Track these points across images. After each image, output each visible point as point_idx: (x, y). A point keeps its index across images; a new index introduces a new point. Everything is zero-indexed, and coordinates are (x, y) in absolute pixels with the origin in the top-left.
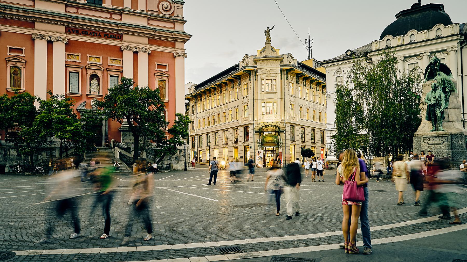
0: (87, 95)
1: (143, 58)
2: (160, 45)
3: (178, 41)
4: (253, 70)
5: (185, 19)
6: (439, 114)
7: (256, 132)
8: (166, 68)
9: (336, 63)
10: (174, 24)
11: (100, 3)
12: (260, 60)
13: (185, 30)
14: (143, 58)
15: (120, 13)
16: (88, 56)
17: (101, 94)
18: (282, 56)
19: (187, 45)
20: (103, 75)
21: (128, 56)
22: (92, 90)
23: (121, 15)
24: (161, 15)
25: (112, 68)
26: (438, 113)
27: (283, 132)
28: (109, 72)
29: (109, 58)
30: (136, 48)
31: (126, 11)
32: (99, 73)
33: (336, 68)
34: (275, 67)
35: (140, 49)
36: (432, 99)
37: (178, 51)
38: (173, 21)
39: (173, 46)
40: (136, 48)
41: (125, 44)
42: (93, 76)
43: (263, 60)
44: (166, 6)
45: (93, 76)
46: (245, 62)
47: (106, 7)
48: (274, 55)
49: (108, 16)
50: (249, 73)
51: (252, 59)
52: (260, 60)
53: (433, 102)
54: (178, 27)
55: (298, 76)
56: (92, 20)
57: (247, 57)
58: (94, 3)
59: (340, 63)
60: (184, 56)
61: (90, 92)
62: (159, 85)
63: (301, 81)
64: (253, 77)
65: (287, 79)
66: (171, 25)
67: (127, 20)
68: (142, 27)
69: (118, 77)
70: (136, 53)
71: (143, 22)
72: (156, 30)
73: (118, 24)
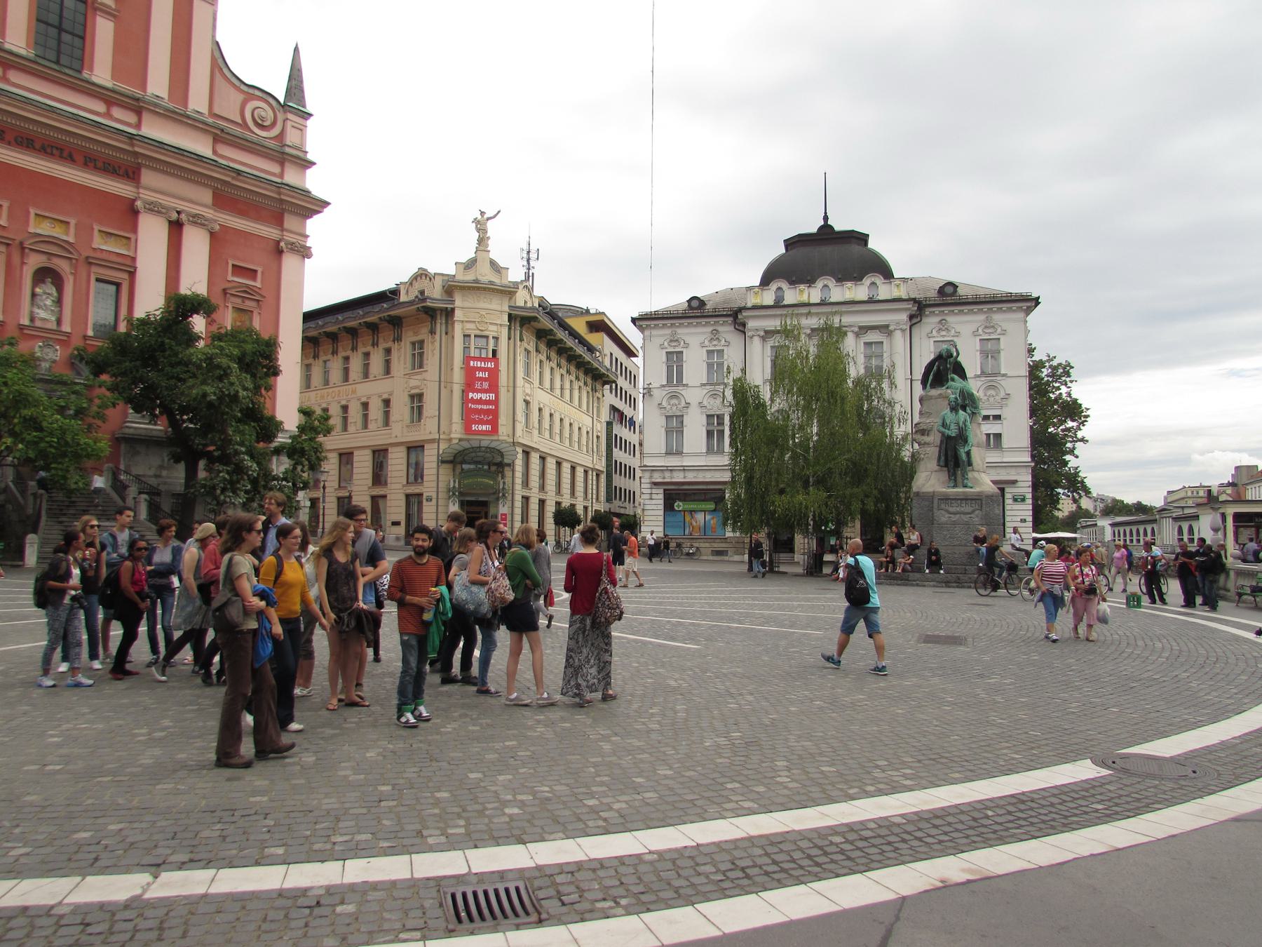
0: (21, 328)
1: (196, 246)
2: (243, 213)
3: (291, 212)
4: (441, 310)
5: (310, 157)
6: (964, 457)
7: (443, 462)
8: (254, 279)
9: (669, 322)
10: (282, 164)
11: (76, 65)
12: (462, 288)
14: (196, 246)
16: (32, 211)
17: (66, 328)
18: (516, 285)
19: (315, 227)
20: (74, 274)
22: (42, 314)
23: (139, 112)
24: (248, 135)
25: (104, 256)
26: (962, 452)
27: (509, 465)
28: (94, 269)
29: (96, 227)
30: (179, 213)
31: (156, 105)
32: (63, 266)
33: (668, 331)
34: (499, 308)
35: (189, 214)
36: (953, 426)
37: (290, 237)
39: (278, 220)
40: (179, 213)
41: (146, 195)
42: (44, 274)
43: (469, 288)
44: (263, 114)
45: (44, 274)
46: (418, 286)
47: (95, 79)
48: (497, 281)
49: (100, 107)
51: (438, 283)
52: (462, 288)
53: (953, 432)
55: (541, 334)
56: (53, 110)
57: (422, 274)
58: (58, 62)
59: (677, 322)
60: (305, 253)
61: (32, 319)
62: (234, 320)
63: (543, 347)
65: (521, 340)
66: (275, 168)
67: (153, 129)
68: (199, 158)
69: (118, 285)
70: (176, 228)
71: (201, 146)
72: (238, 172)
73: (131, 137)
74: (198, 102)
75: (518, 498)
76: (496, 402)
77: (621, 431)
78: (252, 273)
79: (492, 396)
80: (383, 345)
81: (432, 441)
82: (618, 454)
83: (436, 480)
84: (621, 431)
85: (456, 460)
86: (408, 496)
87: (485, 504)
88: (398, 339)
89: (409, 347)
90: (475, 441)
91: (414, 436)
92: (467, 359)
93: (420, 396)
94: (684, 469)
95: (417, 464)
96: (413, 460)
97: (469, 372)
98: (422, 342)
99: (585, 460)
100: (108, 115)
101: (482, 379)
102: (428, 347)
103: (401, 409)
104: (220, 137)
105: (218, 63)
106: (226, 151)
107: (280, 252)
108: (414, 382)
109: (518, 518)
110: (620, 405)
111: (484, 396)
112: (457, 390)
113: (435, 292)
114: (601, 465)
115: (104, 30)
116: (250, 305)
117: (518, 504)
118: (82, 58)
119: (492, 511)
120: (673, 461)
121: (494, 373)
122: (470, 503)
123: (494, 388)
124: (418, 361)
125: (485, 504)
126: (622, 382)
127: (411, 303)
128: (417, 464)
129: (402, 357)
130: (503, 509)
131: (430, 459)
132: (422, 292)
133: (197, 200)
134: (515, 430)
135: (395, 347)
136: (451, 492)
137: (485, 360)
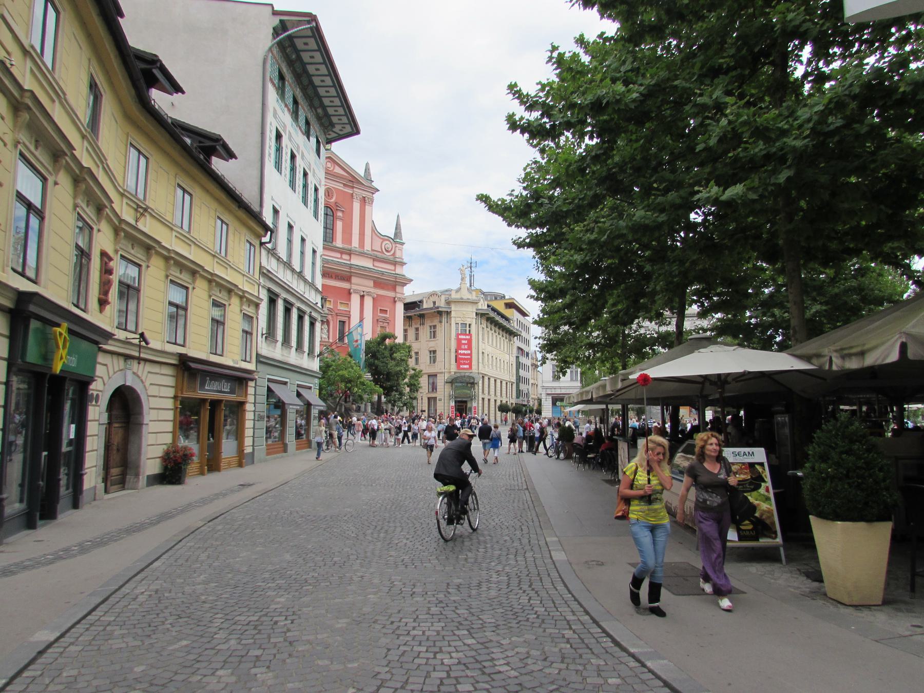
1: (368, 302)
2: (383, 288)
5: (405, 261)
13: (404, 273)
14: (368, 302)
15: (350, 253)
21: (355, 299)
23: (350, 255)
37: (398, 295)
38: (395, 263)
39: (394, 289)
41: (354, 287)
46: (432, 299)
49: (338, 255)
50: (440, 313)
51: (443, 298)
54: (399, 270)
57: (433, 294)
63: (489, 325)
64: (444, 319)
66: (393, 268)
67: (356, 261)
70: (362, 297)
71: (368, 264)
74: (367, 247)
75: (480, 399)
76: (471, 355)
77: (523, 360)
78: (385, 311)
79: (469, 352)
80: (414, 326)
81: (441, 373)
82: (522, 373)
83: (444, 393)
84: (523, 360)
85: (452, 382)
86: (429, 399)
87: (466, 402)
88: (423, 324)
89: (428, 328)
90: (463, 373)
91: (432, 370)
92: (458, 335)
93: (434, 352)
94: (560, 388)
95: (433, 383)
96: (431, 381)
97: (459, 341)
98: (435, 327)
99: (506, 377)
100: (341, 258)
101: (464, 343)
102: (438, 329)
103: (425, 357)
104: (375, 259)
105: (374, 229)
106: (377, 264)
107: (395, 302)
108: (432, 345)
109: (480, 408)
110: (523, 346)
111: (466, 352)
112: (453, 350)
113: (441, 304)
114: (514, 379)
115: (339, 225)
116: (385, 324)
117: (481, 402)
118: (333, 239)
119: (469, 405)
120: (556, 384)
121: (470, 341)
122: (459, 402)
123: (470, 348)
124: (434, 335)
125: (466, 402)
126: (524, 334)
127: (431, 309)
128: (433, 383)
129: (425, 332)
130: (474, 404)
131: (440, 382)
132: (434, 303)
133: (367, 285)
134: (480, 367)
135: (421, 328)
136: (450, 397)
137: (466, 335)
